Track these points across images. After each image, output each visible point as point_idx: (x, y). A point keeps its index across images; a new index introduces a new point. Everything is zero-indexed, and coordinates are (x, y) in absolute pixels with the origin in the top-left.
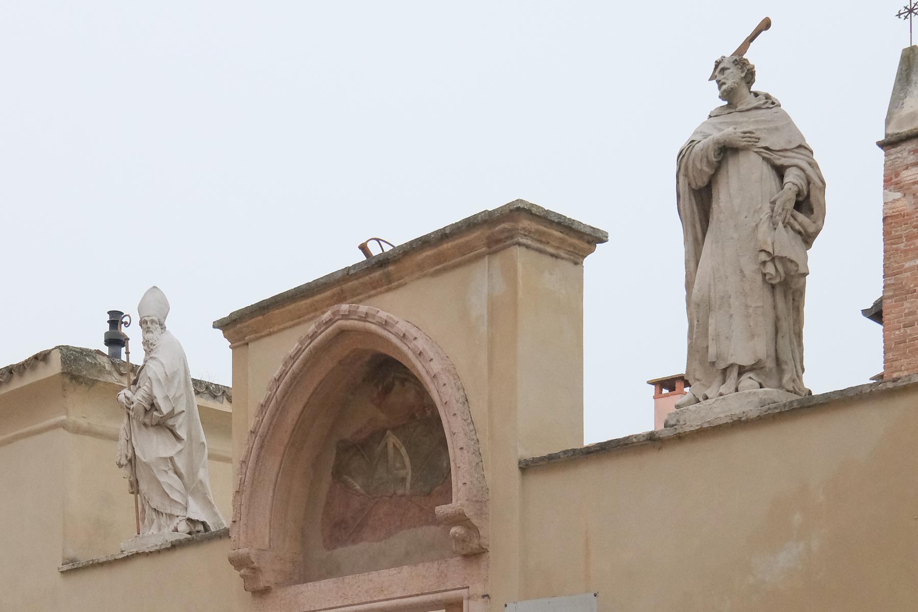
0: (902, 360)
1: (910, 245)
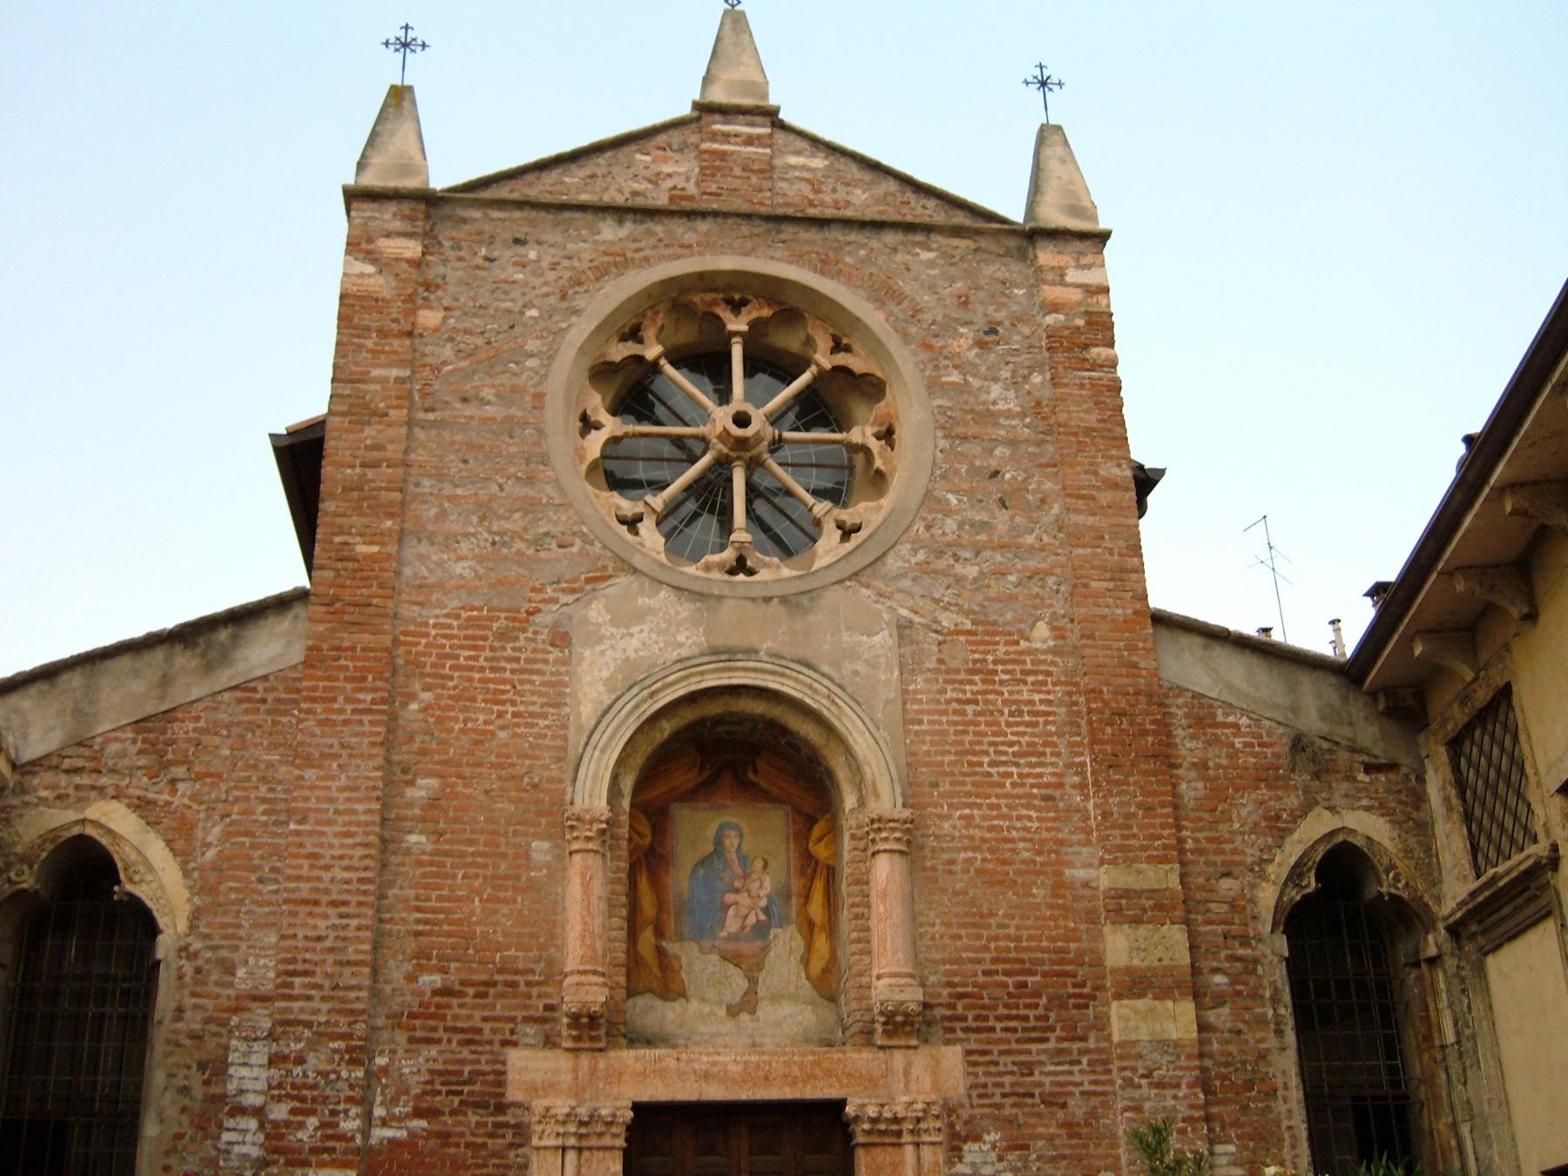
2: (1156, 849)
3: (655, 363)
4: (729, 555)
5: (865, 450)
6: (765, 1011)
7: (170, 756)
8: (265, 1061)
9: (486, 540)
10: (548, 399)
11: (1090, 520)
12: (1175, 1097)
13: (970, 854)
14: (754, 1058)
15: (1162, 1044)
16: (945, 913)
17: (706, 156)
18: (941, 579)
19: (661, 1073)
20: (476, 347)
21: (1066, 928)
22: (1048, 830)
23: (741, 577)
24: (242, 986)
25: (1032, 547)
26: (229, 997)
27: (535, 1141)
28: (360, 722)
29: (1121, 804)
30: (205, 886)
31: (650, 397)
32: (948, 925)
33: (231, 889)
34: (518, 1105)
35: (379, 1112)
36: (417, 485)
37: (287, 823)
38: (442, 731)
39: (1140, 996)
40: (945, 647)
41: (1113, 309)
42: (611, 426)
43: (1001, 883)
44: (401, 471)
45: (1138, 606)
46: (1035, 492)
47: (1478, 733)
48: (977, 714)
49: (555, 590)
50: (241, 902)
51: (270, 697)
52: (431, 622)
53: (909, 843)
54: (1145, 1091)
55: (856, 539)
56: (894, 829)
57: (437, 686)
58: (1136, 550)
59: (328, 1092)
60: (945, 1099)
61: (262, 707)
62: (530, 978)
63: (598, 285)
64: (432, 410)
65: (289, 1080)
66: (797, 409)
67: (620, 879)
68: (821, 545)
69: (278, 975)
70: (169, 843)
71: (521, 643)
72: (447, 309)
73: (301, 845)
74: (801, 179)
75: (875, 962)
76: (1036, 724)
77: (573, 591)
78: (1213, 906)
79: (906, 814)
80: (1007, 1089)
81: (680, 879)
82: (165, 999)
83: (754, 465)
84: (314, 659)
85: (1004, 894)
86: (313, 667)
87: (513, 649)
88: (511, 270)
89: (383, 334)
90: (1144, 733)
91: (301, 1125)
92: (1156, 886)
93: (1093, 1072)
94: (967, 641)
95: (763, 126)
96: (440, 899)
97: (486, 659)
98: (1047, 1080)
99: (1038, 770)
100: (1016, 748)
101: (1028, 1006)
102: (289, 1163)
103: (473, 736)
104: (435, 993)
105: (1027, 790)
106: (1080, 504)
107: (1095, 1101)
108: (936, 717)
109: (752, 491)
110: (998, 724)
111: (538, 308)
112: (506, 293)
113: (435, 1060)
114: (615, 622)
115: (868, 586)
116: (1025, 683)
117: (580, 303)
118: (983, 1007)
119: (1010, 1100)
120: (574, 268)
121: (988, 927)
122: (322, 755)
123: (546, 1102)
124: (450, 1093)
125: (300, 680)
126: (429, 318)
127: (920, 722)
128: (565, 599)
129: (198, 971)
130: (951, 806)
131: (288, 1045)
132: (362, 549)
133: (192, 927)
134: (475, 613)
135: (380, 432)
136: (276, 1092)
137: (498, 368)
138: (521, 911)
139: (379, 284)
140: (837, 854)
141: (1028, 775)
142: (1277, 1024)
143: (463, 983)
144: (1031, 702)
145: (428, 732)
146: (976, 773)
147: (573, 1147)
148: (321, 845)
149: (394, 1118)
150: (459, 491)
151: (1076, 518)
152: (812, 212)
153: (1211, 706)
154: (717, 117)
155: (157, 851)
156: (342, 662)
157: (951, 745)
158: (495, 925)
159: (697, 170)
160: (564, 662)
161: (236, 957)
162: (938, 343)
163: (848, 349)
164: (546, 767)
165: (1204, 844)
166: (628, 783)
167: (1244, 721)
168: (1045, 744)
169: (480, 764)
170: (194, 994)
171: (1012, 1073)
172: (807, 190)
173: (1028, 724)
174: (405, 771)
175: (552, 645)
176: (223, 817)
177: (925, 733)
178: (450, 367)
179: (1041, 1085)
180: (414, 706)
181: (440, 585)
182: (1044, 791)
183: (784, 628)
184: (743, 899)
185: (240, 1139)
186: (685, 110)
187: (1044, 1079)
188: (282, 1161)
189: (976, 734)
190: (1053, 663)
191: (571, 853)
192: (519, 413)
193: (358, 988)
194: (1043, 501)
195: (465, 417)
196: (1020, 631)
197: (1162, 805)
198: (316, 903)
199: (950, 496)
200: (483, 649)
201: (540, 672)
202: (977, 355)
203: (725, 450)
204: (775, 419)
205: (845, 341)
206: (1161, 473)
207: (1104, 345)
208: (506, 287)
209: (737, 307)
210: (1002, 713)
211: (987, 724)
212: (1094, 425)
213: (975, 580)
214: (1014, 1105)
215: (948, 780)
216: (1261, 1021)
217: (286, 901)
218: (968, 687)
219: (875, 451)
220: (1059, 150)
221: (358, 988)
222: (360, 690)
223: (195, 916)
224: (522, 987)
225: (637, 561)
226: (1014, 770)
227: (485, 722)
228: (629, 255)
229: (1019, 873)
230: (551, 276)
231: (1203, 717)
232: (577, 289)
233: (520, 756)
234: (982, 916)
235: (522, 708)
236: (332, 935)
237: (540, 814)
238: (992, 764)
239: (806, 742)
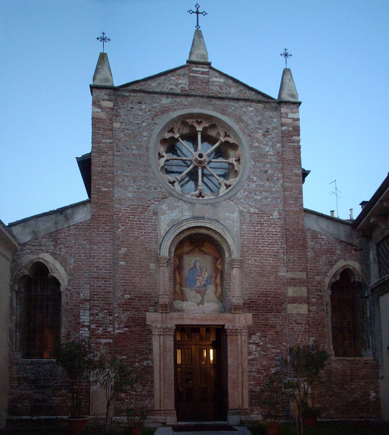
0: (101, 181)
1: (105, 133)
2: (301, 268)
4: (197, 192)
5: (232, 164)
6: (206, 304)
7: (59, 242)
8: (89, 315)
9: (135, 187)
10: (150, 150)
12: (301, 327)
13: (256, 269)
14: (204, 315)
15: (298, 314)
17: (191, 78)
21: (278, 287)
22: (275, 263)
23: (200, 198)
24: (82, 298)
25: (274, 191)
26: (79, 300)
27: (153, 333)
29: (293, 257)
30: (71, 274)
31: (176, 148)
32: (250, 285)
33: (77, 275)
34: (149, 325)
35: (117, 326)
36: (117, 172)
39: (295, 303)
41: (300, 125)
42: (167, 156)
43: (263, 276)
44: (112, 168)
46: (276, 177)
47: (384, 242)
48: (259, 234)
49: (153, 201)
53: (241, 265)
54: (294, 325)
55: (230, 188)
57: (125, 225)
58: (301, 193)
60: (247, 325)
61: (81, 230)
63: (162, 116)
64: (119, 151)
66: (215, 152)
67: (172, 273)
68: (221, 190)
69: (91, 295)
70: (61, 264)
71: (146, 214)
72: (121, 123)
73: (94, 264)
74: (217, 85)
76: (273, 237)
77: (158, 201)
78: (314, 282)
79: (241, 259)
80: (262, 324)
81: (186, 273)
82: (64, 299)
83: (203, 168)
88: (138, 111)
89: (105, 130)
90: (300, 240)
91: (99, 330)
92: (300, 278)
93: (282, 320)
95: (206, 68)
97: (137, 219)
99: (273, 249)
100: (268, 243)
102: (96, 338)
103: (135, 238)
104: (129, 299)
105: (270, 253)
107: (283, 327)
108: (248, 235)
109: (203, 175)
110: (264, 237)
112: (137, 118)
113: (129, 315)
114: (169, 209)
115: (232, 201)
116: (271, 227)
117: (157, 121)
122: (98, 242)
123: (156, 325)
124: (133, 322)
125: (90, 223)
126: (116, 125)
127: (244, 236)
129: (71, 294)
130: (251, 257)
131: (94, 311)
132: (104, 189)
133: (68, 284)
134: (134, 207)
137: (136, 140)
139: (102, 115)
141: (270, 250)
142: (327, 311)
143: (135, 297)
144: (272, 232)
146: (258, 249)
147: (162, 335)
149: (120, 328)
150: (128, 174)
151: (286, 184)
152: (220, 95)
153: (317, 234)
154: (194, 65)
155: (58, 265)
156: (100, 219)
157: (252, 242)
159: (188, 82)
160: (156, 220)
161: (80, 291)
162: (252, 135)
163: (228, 136)
164: (153, 246)
165: (313, 267)
166: (173, 250)
167: (325, 237)
168: (275, 242)
169: (137, 245)
170: (70, 300)
171: (264, 320)
172: (218, 89)
173: (271, 237)
175: (153, 215)
177: (246, 239)
178: (123, 140)
180: (119, 230)
182: (274, 254)
184: (201, 278)
185: (84, 333)
186: (184, 63)
187: (272, 321)
188: (94, 337)
189: (258, 239)
190: (278, 222)
191: (160, 267)
192: (142, 153)
194: (278, 179)
195: (128, 154)
197: (303, 258)
198: (99, 278)
199: (254, 177)
202: (263, 138)
203: (196, 164)
204: (209, 155)
205: (228, 134)
206: (309, 172)
207: (297, 136)
208: (137, 117)
209: (199, 123)
210: (265, 234)
211: (261, 237)
212: (293, 158)
213: (259, 200)
214: (264, 327)
215: (251, 250)
216: (323, 310)
217: (91, 278)
218: (256, 228)
220: (289, 77)
222: (106, 226)
223: (69, 281)
224: (149, 298)
225: (174, 193)
226: (267, 248)
228: (170, 108)
229: (267, 273)
230: (149, 113)
231: (315, 236)
233: (146, 243)
234: (258, 283)
235: (146, 231)
237: (152, 257)
238: (262, 247)
239: (216, 241)
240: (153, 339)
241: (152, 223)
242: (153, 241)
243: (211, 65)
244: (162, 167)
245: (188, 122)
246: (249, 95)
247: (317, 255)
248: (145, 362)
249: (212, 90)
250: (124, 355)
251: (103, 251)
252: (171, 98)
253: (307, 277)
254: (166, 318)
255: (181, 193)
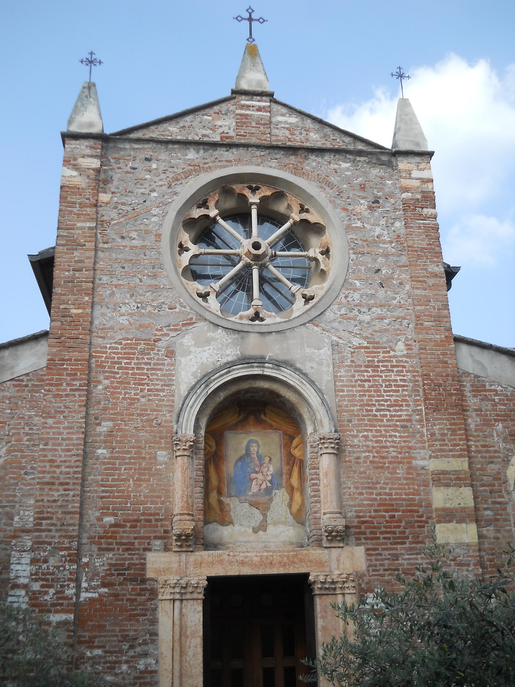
0: (70, 296)
1: (82, 211)
2: (457, 451)
3: (214, 219)
4: (251, 312)
5: (316, 260)
9: (134, 306)
11: (424, 293)
12: (467, 570)
13: (368, 454)
14: (266, 554)
15: (460, 545)
16: (355, 482)
17: (238, 117)
18: (352, 322)
19: (221, 562)
20: (128, 211)
21: (414, 489)
22: (405, 442)
23: (257, 322)
24: (17, 525)
25: (396, 306)
26: (10, 530)
27: (160, 597)
28: (74, 395)
29: (440, 429)
31: (213, 234)
32: (357, 488)
33: (11, 478)
34: (152, 579)
35: (84, 585)
37: (38, 445)
38: (114, 398)
39: (450, 521)
40: (354, 355)
42: (194, 249)
43: (382, 467)
45: (447, 334)
46: (397, 279)
48: (370, 387)
50: (16, 484)
51: (30, 384)
52: (108, 346)
54: (453, 567)
55: (312, 303)
56: (331, 443)
57: (111, 377)
58: (446, 306)
59: (60, 576)
61: (26, 389)
62: (157, 517)
63: (186, 181)
65: (41, 571)
66: (284, 239)
67: (200, 468)
69: (35, 520)
72: (113, 193)
73: (45, 456)
74: (284, 128)
75: (323, 506)
76: (398, 391)
77: (176, 330)
78: (485, 478)
79: (336, 435)
83: (262, 268)
84: (51, 364)
85: (383, 473)
86: (51, 369)
87: (147, 359)
88: (144, 173)
90: (451, 395)
91: (46, 593)
94: (365, 352)
95: (266, 102)
96: (113, 480)
97: (135, 364)
98: (405, 562)
99: (399, 413)
100: (389, 403)
101: (395, 527)
102: (41, 611)
103: (129, 401)
104: (111, 526)
105: (394, 423)
106: (419, 285)
108: (350, 388)
109: (262, 280)
110: (380, 391)
111: (157, 192)
113: (111, 559)
114: (198, 344)
115: (317, 326)
116: (393, 371)
117: (178, 189)
118: (374, 527)
119: (387, 573)
120: (175, 172)
121: (376, 488)
122: (56, 412)
123: (165, 578)
124: (119, 575)
125: (44, 375)
127: (343, 391)
128: (172, 334)
130: (358, 431)
131: (39, 554)
132: (74, 311)
134: (129, 342)
135: (81, 253)
136: (35, 577)
137: (138, 222)
138: (152, 485)
140: (304, 454)
141: (394, 416)
143: (124, 521)
144: (396, 381)
145: (107, 399)
146: (370, 415)
147: (178, 599)
148: (55, 456)
149: (92, 587)
150: (120, 282)
152: (289, 143)
153: (483, 381)
156: (65, 366)
157: (357, 401)
158: (140, 492)
159: (234, 124)
160: (172, 365)
161: (14, 511)
162: (350, 208)
163: (307, 211)
164: (164, 415)
165: (480, 448)
167: (500, 388)
168: (403, 401)
169: (132, 415)
172: (287, 133)
173: (394, 391)
174: (96, 419)
176: (7, 443)
178: (115, 221)
179: (402, 565)
180: (100, 387)
181: (112, 328)
182: (402, 423)
183: (278, 347)
185: (17, 600)
186: (228, 94)
188: (37, 610)
189: (370, 396)
190: (406, 362)
191: (176, 457)
192: (149, 244)
193: (74, 525)
194: (401, 284)
195: (123, 246)
196: (390, 347)
197: (460, 429)
198: (53, 484)
199: (356, 282)
200: (133, 359)
201: (161, 369)
202: (369, 214)
203: (249, 261)
204: (273, 245)
205: (306, 207)
206: (458, 269)
208: (142, 182)
209: (254, 190)
210: (382, 386)
211: (375, 391)
213: (368, 323)
214: (390, 575)
215: (356, 418)
218: (365, 374)
219: (320, 260)
221: (74, 525)
225: (207, 315)
226: (388, 413)
227: (135, 394)
228: (201, 165)
229: (390, 463)
230: (163, 176)
232: (176, 182)
234: (373, 483)
235: (152, 387)
236: (61, 499)
237: (161, 438)
238: (377, 410)
239: (288, 400)
240: (159, 609)
241: (164, 372)
242: (165, 405)
243: (274, 97)
244: (186, 269)
245: (234, 189)
246: (341, 143)
247: (487, 423)
248: (142, 662)
249: (277, 136)
250: (99, 647)
251: (65, 428)
252: (204, 149)
253: (470, 467)
254: (187, 563)
255: (220, 315)
